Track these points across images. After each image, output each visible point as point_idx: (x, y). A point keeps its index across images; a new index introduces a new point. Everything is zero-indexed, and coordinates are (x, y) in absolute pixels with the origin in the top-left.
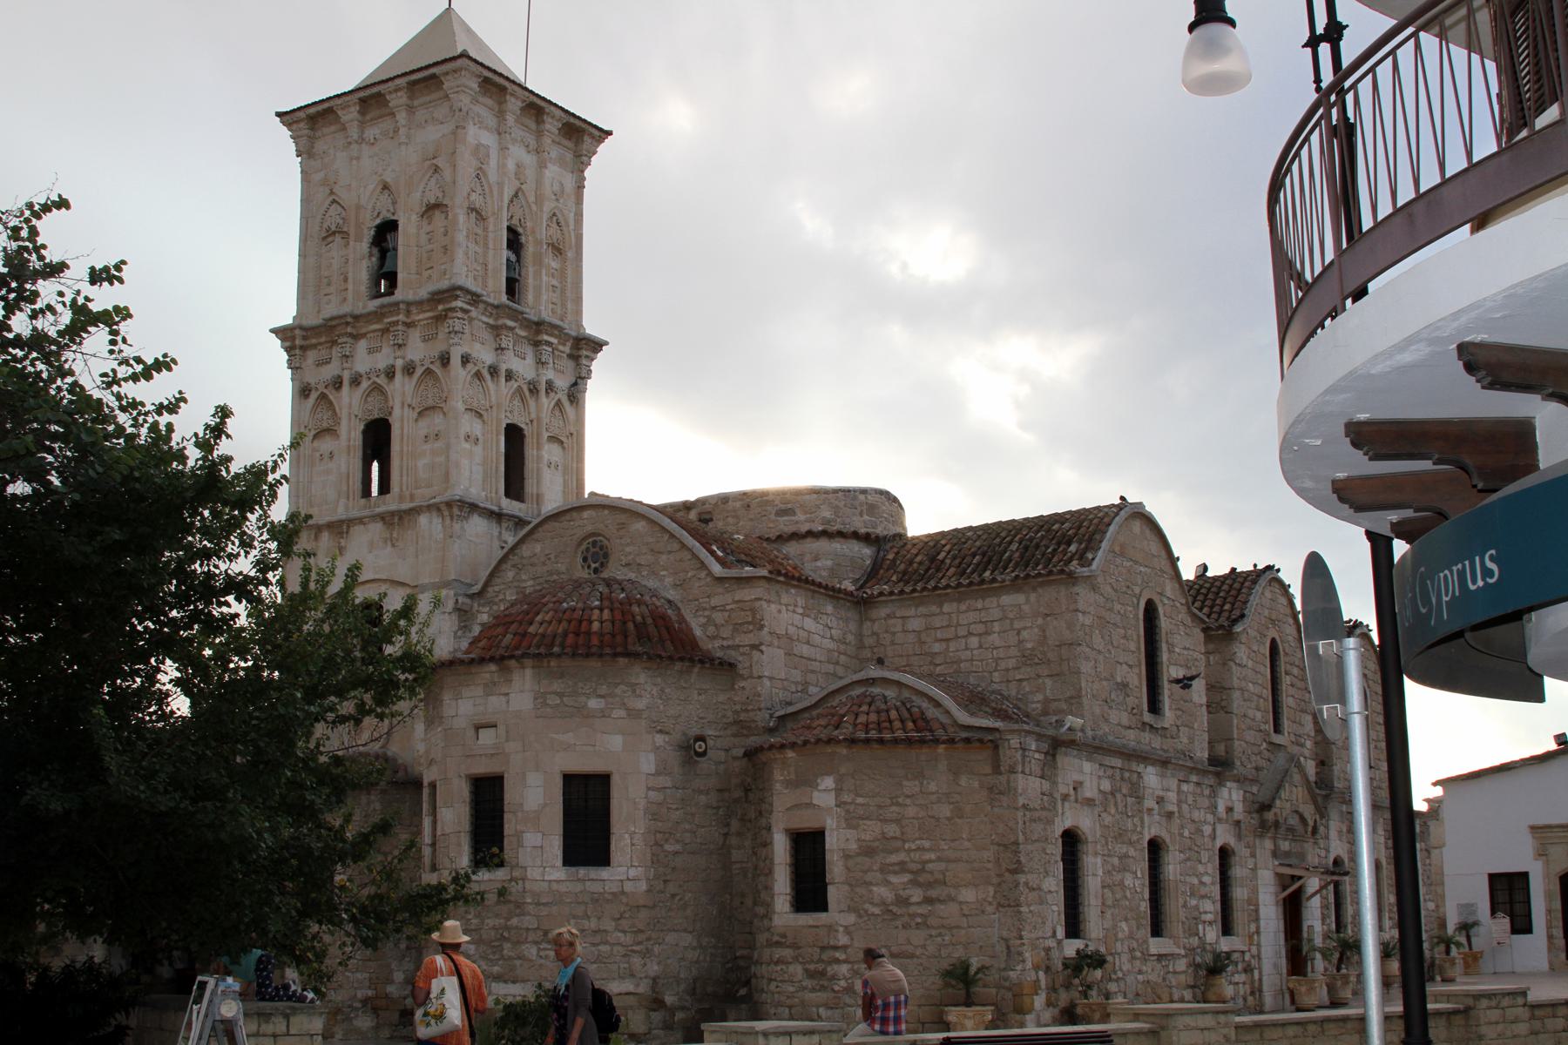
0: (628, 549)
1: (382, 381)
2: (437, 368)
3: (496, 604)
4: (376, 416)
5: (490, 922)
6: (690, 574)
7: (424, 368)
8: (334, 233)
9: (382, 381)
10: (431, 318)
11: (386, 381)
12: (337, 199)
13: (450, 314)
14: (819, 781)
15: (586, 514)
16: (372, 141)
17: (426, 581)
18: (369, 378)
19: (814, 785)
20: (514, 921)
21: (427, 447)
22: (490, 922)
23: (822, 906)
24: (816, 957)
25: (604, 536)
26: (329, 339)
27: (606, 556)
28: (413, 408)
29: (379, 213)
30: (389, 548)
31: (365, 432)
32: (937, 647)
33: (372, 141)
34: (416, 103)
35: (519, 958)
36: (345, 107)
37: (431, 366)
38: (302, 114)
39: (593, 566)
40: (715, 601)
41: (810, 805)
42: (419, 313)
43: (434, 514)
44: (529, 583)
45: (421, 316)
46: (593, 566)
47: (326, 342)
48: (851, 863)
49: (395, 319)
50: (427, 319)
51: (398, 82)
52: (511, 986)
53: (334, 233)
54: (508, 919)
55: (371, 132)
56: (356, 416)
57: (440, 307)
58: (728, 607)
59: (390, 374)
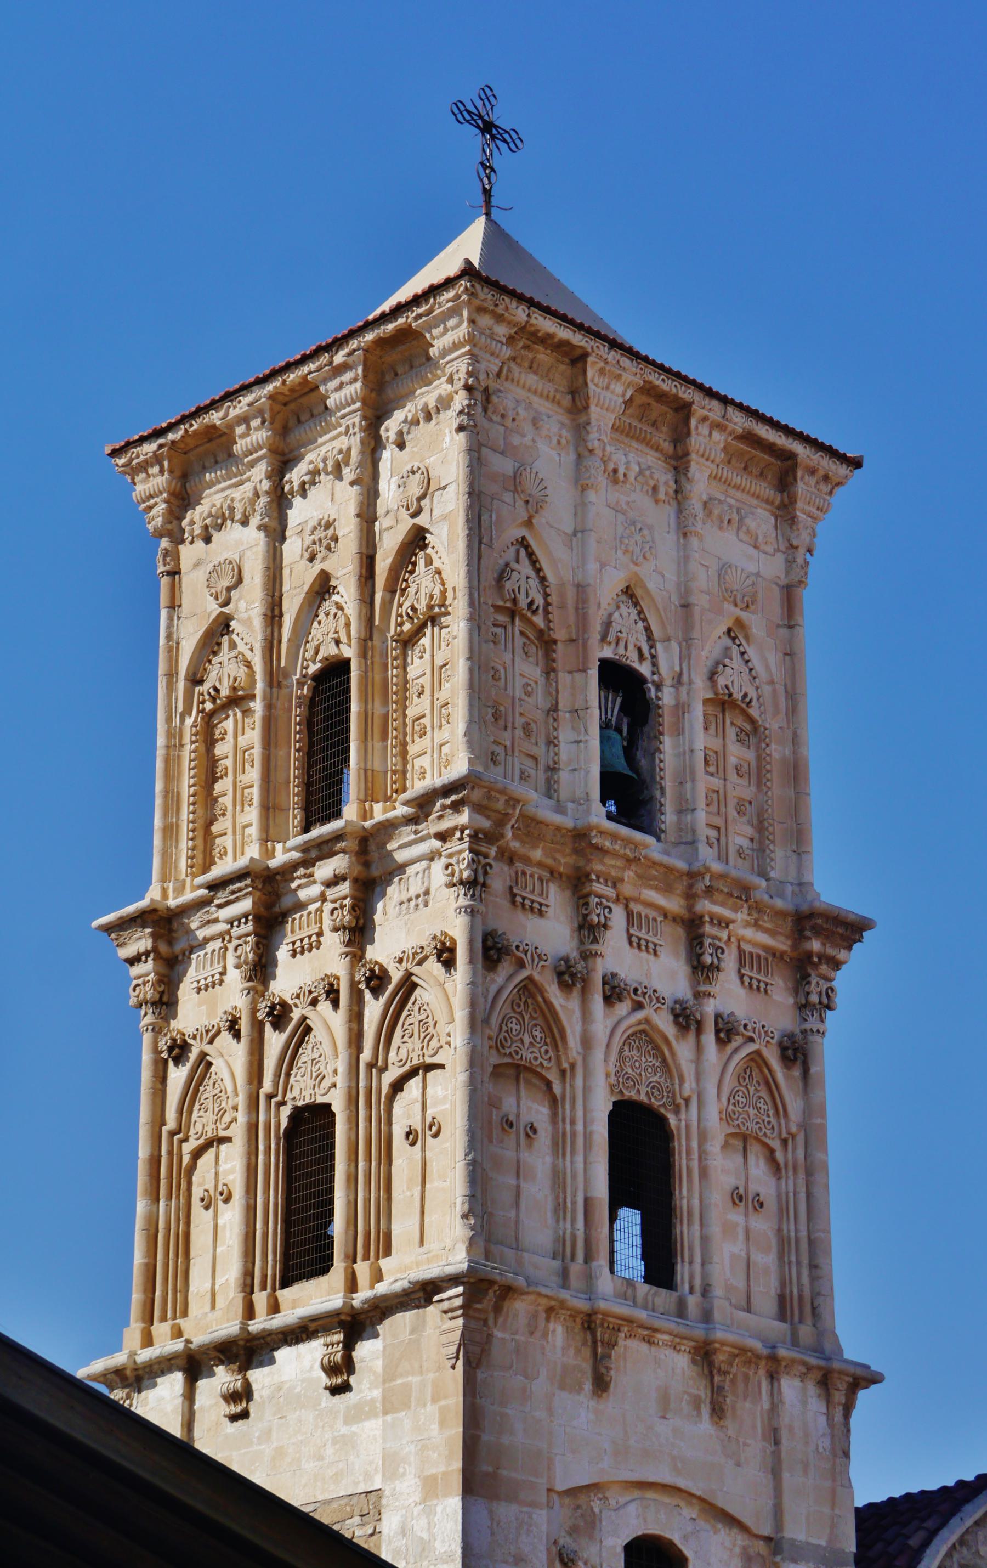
4: (643, 1098)
7: (752, 1047)
10: (766, 948)
12: (532, 542)
13: (824, 968)
26: (549, 861)
30: (706, 1425)
33: (621, 477)
38: (520, 313)
42: (747, 924)
43: (812, 1389)
45: (749, 933)
47: (540, 865)
49: (726, 913)
50: (755, 944)
57: (816, 945)
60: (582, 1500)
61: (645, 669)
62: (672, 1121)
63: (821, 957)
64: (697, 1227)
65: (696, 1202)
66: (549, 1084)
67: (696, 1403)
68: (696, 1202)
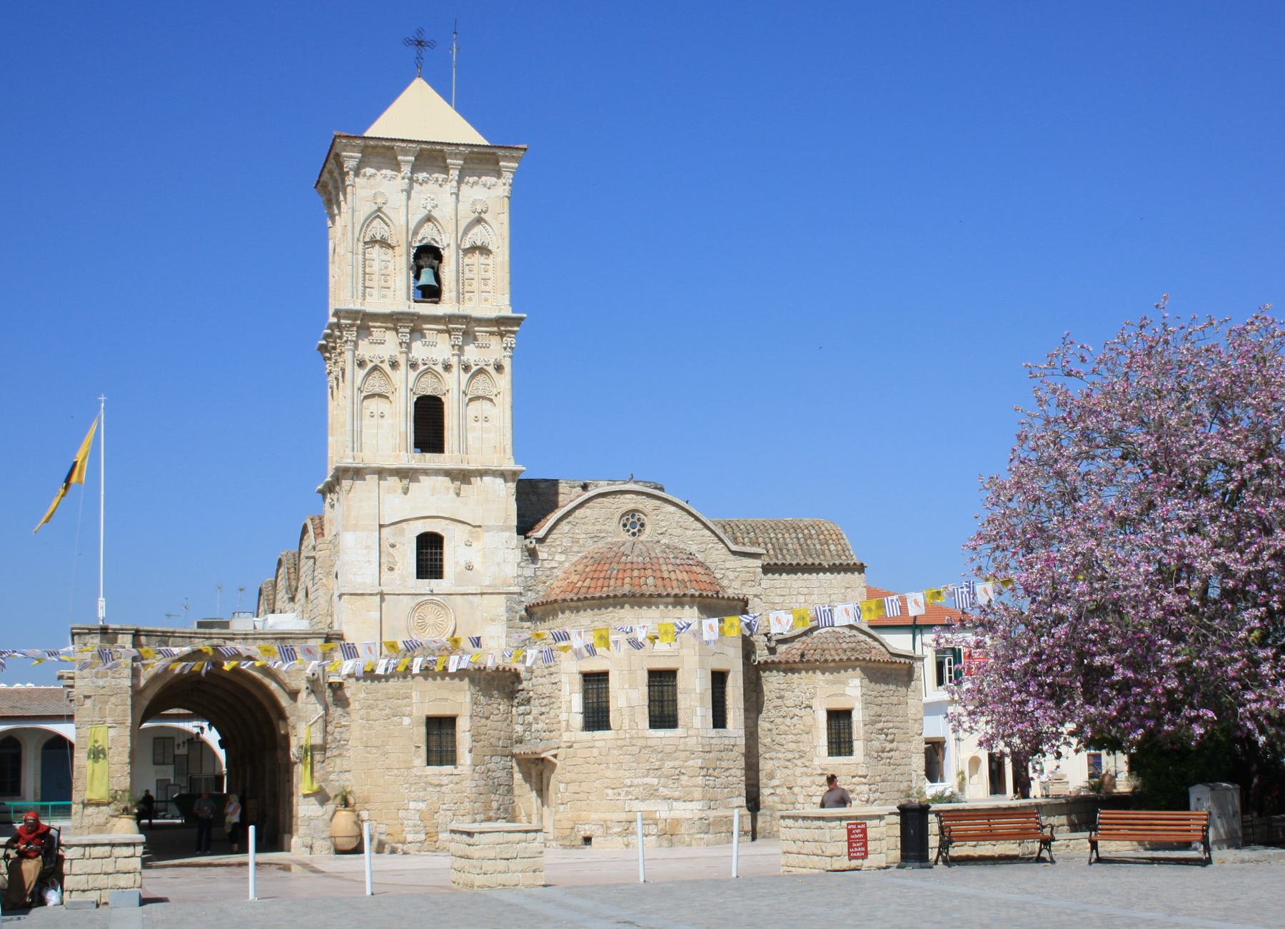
0: (663, 524)
1: (439, 368)
2: (491, 369)
3: (554, 547)
4: (429, 393)
5: (671, 764)
6: (710, 546)
8: (376, 242)
9: (439, 368)
11: (442, 369)
14: (850, 681)
15: (628, 496)
16: (420, 181)
17: (491, 523)
18: (425, 364)
19: (845, 683)
20: (691, 763)
21: (478, 424)
22: (671, 764)
23: (850, 753)
24: (848, 782)
25: (644, 514)
27: (642, 525)
28: (466, 395)
29: (423, 238)
30: (452, 494)
31: (416, 403)
32: (778, 600)
34: (466, 166)
35: (695, 786)
36: (405, 152)
37: (485, 367)
39: (632, 531)
40: (728, 565)
41: (843, 695)
44: (582, 536)
46: (632, 531)
48: (866, 728)
51: (461, 148)
52: (688, 803)
53: (376, 242)
54: (686, 761)
55: (422, 176)
56: (411, 390)
57: (502, 328)
58: (738, 570)
59: (447, 367)
60: (399, 525)
61: (440, 246)
62: (443, 399)
63: (505, 331)
64: (450, 432)
65: (450, 425)
66: (387, 397)
67: (448, 489)
68: (450, 425)
